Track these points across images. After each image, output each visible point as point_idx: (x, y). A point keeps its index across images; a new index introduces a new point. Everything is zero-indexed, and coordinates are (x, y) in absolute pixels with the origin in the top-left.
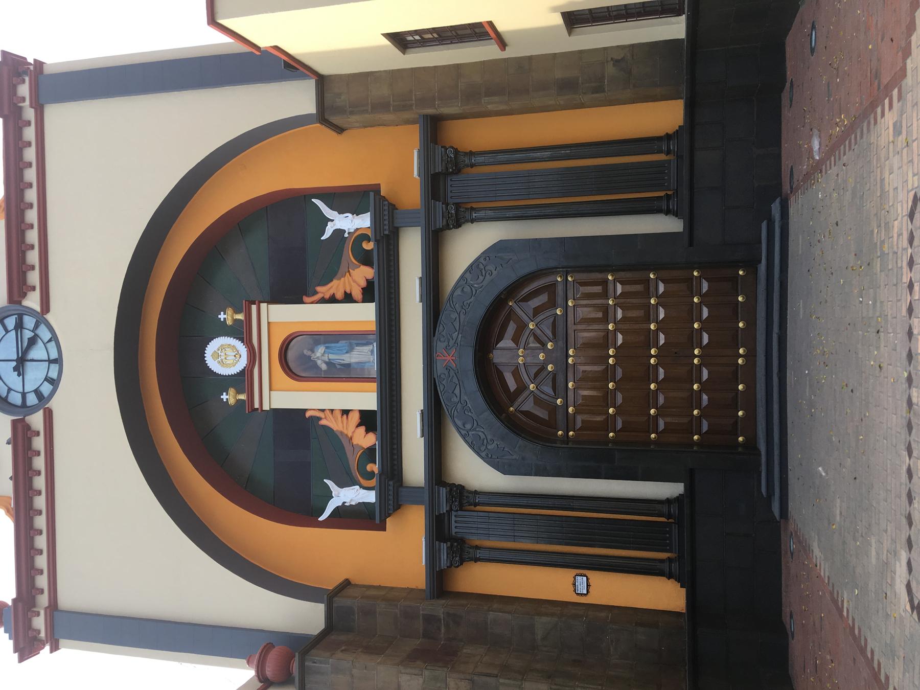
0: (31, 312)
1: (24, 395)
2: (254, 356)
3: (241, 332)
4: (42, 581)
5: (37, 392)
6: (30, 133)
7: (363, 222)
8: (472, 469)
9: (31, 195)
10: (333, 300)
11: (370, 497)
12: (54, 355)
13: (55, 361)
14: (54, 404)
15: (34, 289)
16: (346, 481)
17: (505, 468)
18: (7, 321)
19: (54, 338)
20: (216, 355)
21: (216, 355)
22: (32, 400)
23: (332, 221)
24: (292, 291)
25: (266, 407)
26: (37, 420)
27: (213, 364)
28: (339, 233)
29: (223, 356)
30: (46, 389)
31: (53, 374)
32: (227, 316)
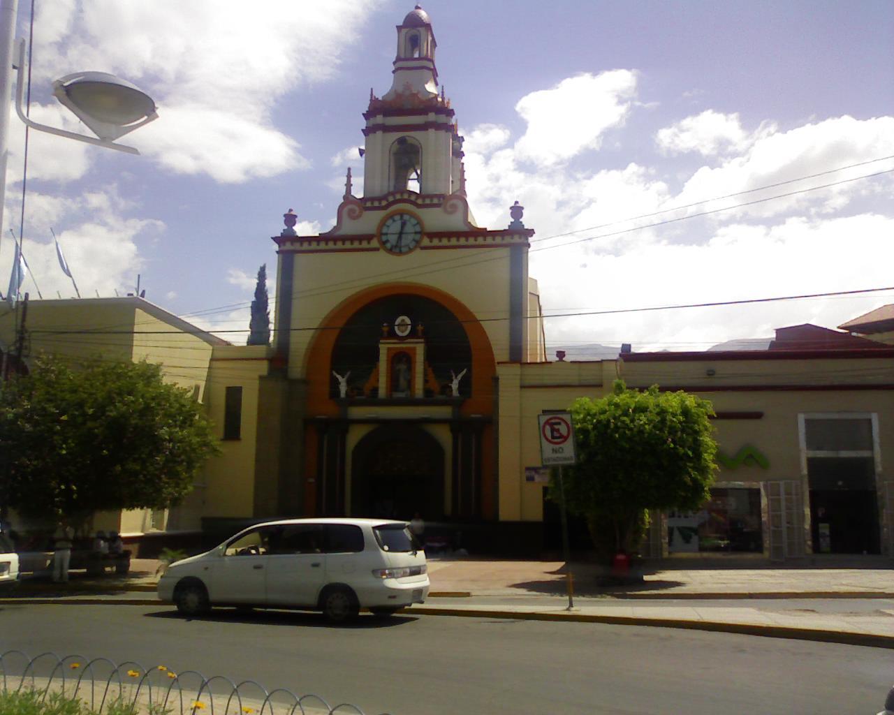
0: (421, 239)
1: (386, 234)
2: (402, 339)
3: (413, 334)
4: (306, 246)
5: (387, 241)
6: (498, 240)
7: (455, 393)
8: (355, 436)
9: (471, 241)
10: (426, 375)
11: (343, 394)
12: (404, 250)
13: (401, 251)
14: (382, 252)
15: (431, 242)
16: (349, 382)
17: (354, 453)
18: (418, 226)
19: (411, 250)
20: (403, 320)
21: (403, 320)
22: (384, 238)
23: (456, 376)
24: (429, 358)
25: (380, 346)
26: (375, 243)
27: (398, 321)
28: (452, 381)
29: (403, 324)
30: (389, 246)
31: (394, 250)
32: (420, 328)
